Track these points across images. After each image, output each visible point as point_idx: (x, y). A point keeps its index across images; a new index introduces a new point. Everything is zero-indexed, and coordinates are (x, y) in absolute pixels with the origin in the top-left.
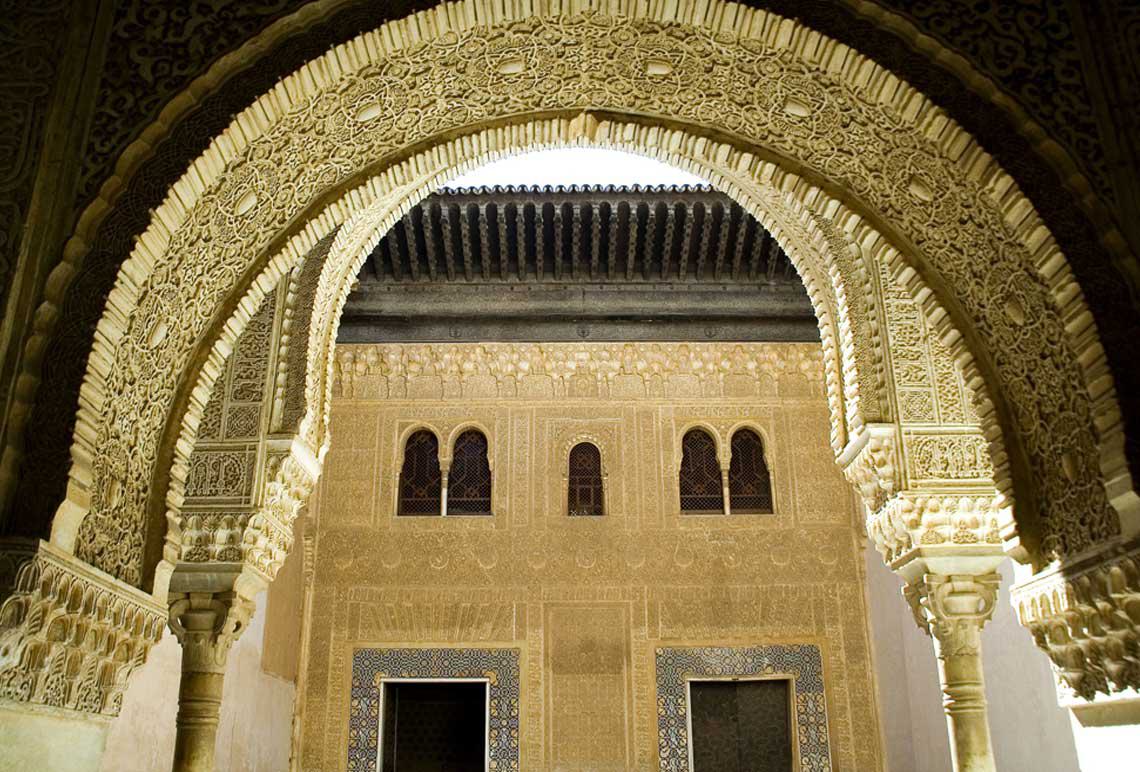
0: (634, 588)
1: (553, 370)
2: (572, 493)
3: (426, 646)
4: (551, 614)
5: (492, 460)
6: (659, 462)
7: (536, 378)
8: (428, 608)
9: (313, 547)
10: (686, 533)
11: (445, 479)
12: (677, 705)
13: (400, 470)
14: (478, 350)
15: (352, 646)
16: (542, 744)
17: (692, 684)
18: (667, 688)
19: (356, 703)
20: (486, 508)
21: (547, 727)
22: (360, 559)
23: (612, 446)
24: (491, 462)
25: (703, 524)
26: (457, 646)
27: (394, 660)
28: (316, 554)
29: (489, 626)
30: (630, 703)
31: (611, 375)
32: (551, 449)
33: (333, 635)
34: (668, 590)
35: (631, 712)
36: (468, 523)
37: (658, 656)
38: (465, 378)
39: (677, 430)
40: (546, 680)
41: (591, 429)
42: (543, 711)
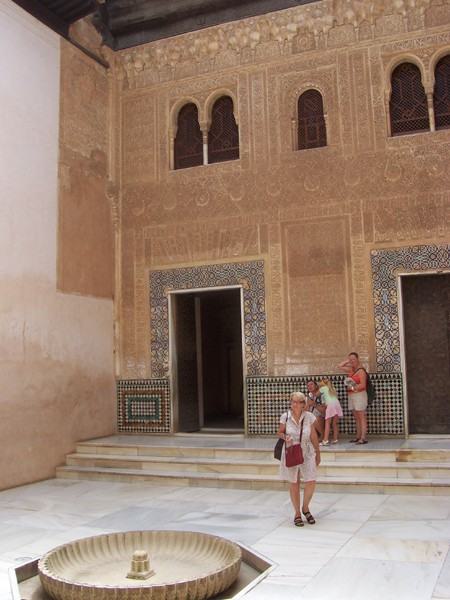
0: (351, 203)
1: (277, 35)
2: (301, 132)
3: (197, 264)
4: (286, 231)
5: (237, 117)
6: (369, 95)
7: (266, 44)
8: (197, 236)
9: (117, 202)
10: (395, 152)
11: (205, 137)
12: (390, 296)
13: (172, 135)
14: (220, 31)
15: (147, 271)
16: (283, 331)
17: (403, 278)
18: (386, 283)
19: (153, 310)
20: (235, 155)
21: (287, 319)
22: (149, 206)
23: (330, 89)
24: (236, 118)
25: (409, 142)
26: (218, 262)
27: (175, 277)
28: (120, 207)
29: (240, 245)
30: (351, 296)
31: (325, 29)
32: (281, 100)
33: (135, 263)
34: (380, 202)
35: (351, 303)
36: (223, 168)
37: (373, 257)
38: (212, 56)
39: (385, 65)
40: (285, 283)
41: (313, 78)
42: (283, 308)
